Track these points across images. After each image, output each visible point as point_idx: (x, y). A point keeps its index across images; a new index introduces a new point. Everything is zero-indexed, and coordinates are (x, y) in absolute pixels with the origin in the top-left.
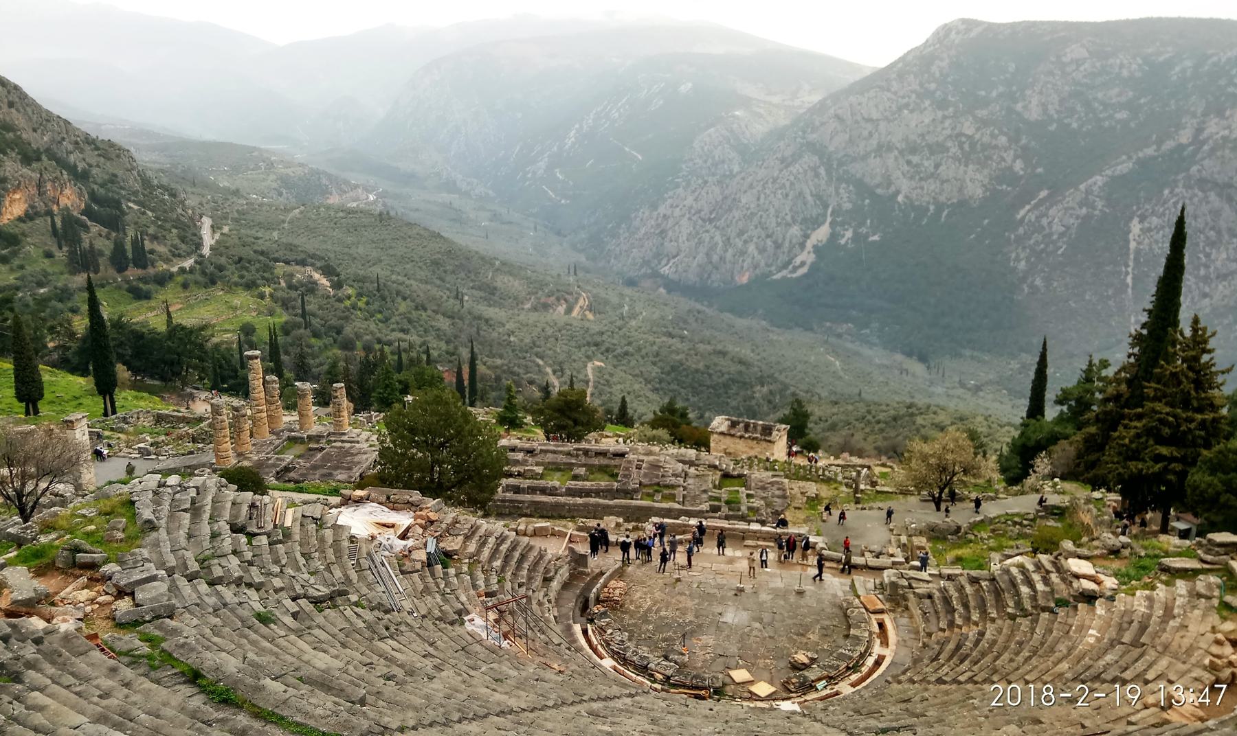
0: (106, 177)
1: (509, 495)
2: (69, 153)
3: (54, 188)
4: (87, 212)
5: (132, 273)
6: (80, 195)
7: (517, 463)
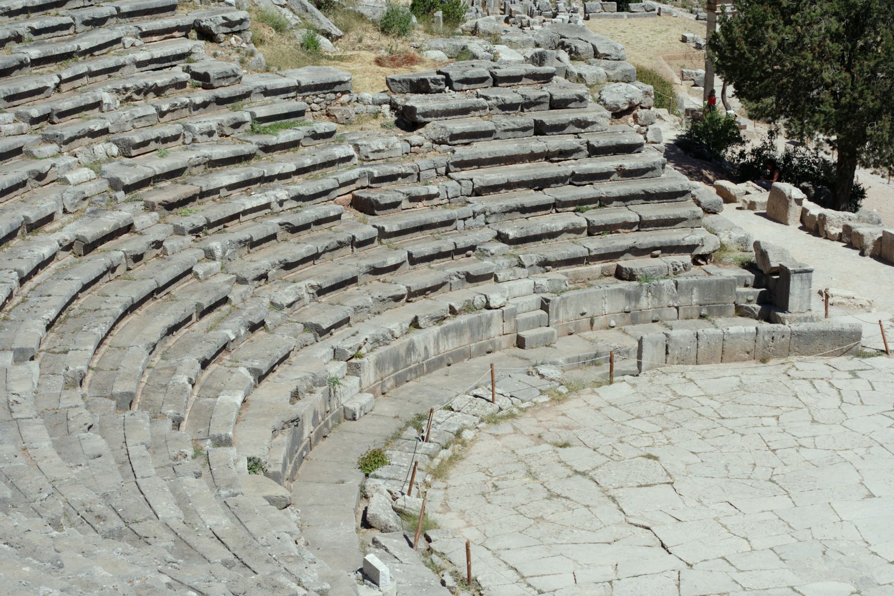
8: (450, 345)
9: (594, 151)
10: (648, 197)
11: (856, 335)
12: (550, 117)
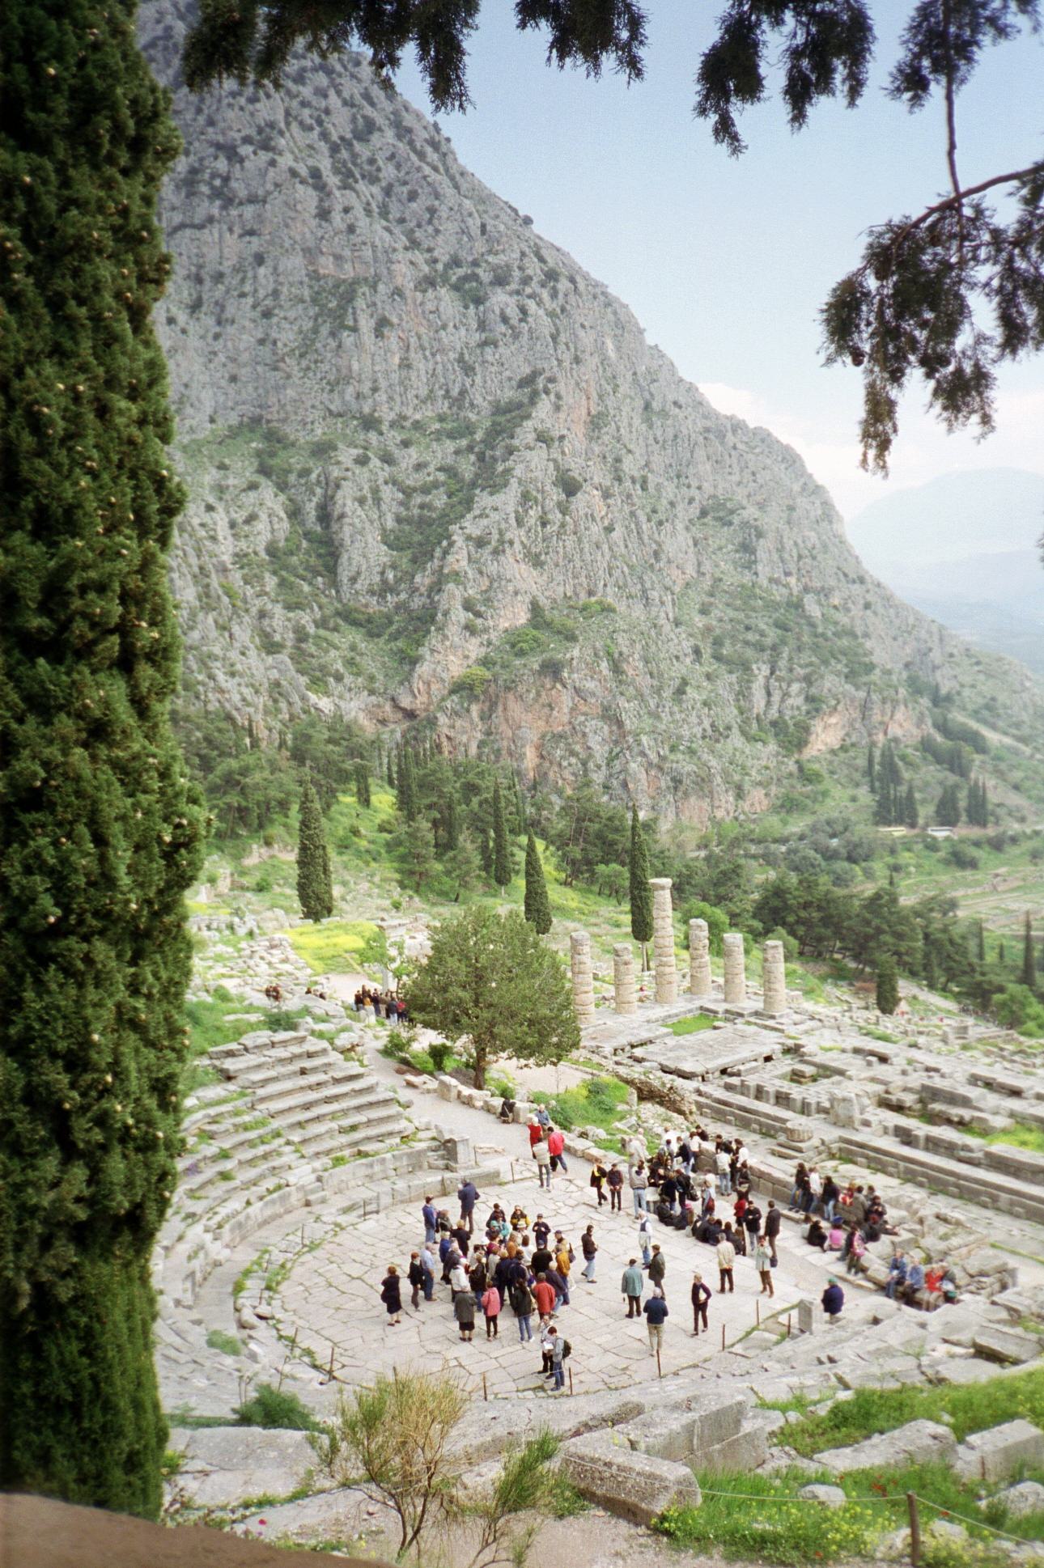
0: (981, 701)
1: (890, 1144)
2: (935, 668)
3: (883, 714)
4: (926, 746)
5: (964, 831)
6: (920, 721)
7: (965, 1102)
8: (268, 1212)
9: (337, 1081)
10: (371, 1105)
11: (497, 1174)
12: (307, 1064)
